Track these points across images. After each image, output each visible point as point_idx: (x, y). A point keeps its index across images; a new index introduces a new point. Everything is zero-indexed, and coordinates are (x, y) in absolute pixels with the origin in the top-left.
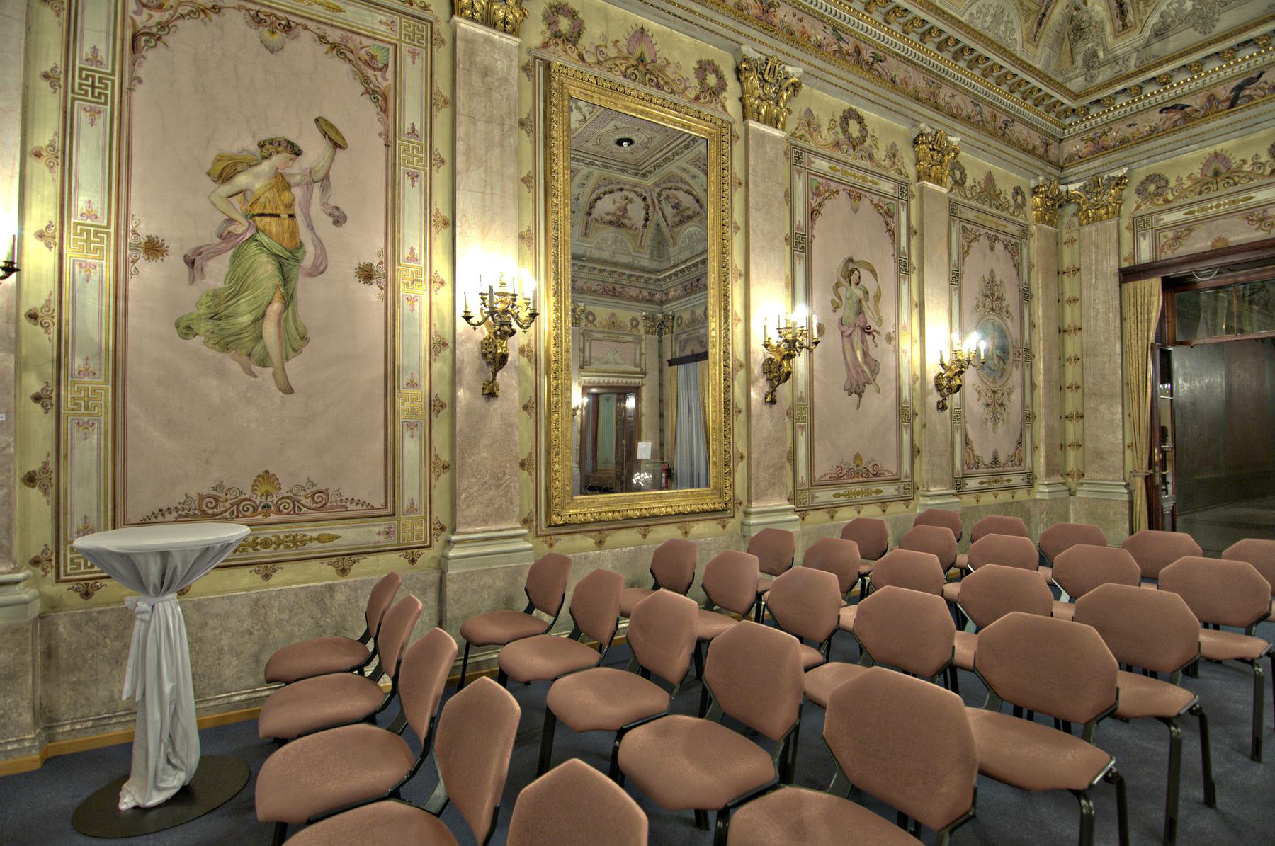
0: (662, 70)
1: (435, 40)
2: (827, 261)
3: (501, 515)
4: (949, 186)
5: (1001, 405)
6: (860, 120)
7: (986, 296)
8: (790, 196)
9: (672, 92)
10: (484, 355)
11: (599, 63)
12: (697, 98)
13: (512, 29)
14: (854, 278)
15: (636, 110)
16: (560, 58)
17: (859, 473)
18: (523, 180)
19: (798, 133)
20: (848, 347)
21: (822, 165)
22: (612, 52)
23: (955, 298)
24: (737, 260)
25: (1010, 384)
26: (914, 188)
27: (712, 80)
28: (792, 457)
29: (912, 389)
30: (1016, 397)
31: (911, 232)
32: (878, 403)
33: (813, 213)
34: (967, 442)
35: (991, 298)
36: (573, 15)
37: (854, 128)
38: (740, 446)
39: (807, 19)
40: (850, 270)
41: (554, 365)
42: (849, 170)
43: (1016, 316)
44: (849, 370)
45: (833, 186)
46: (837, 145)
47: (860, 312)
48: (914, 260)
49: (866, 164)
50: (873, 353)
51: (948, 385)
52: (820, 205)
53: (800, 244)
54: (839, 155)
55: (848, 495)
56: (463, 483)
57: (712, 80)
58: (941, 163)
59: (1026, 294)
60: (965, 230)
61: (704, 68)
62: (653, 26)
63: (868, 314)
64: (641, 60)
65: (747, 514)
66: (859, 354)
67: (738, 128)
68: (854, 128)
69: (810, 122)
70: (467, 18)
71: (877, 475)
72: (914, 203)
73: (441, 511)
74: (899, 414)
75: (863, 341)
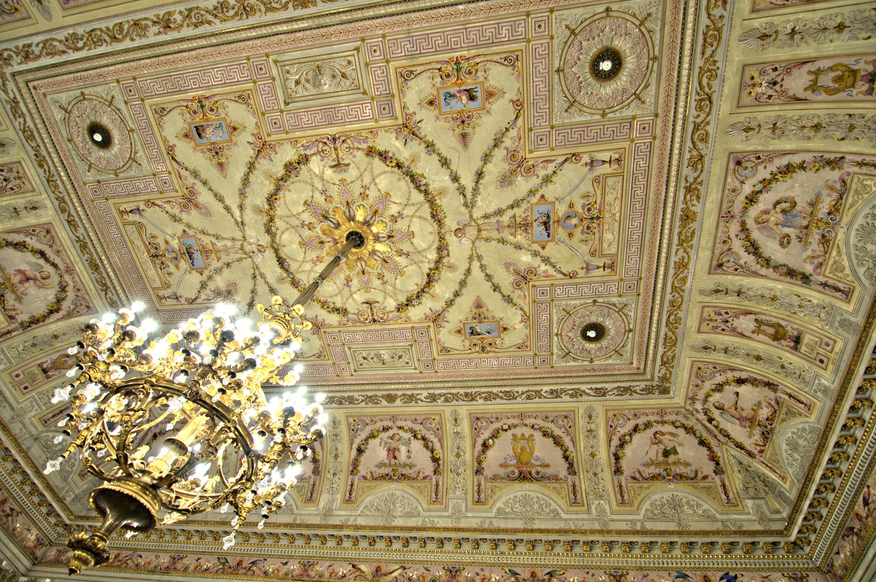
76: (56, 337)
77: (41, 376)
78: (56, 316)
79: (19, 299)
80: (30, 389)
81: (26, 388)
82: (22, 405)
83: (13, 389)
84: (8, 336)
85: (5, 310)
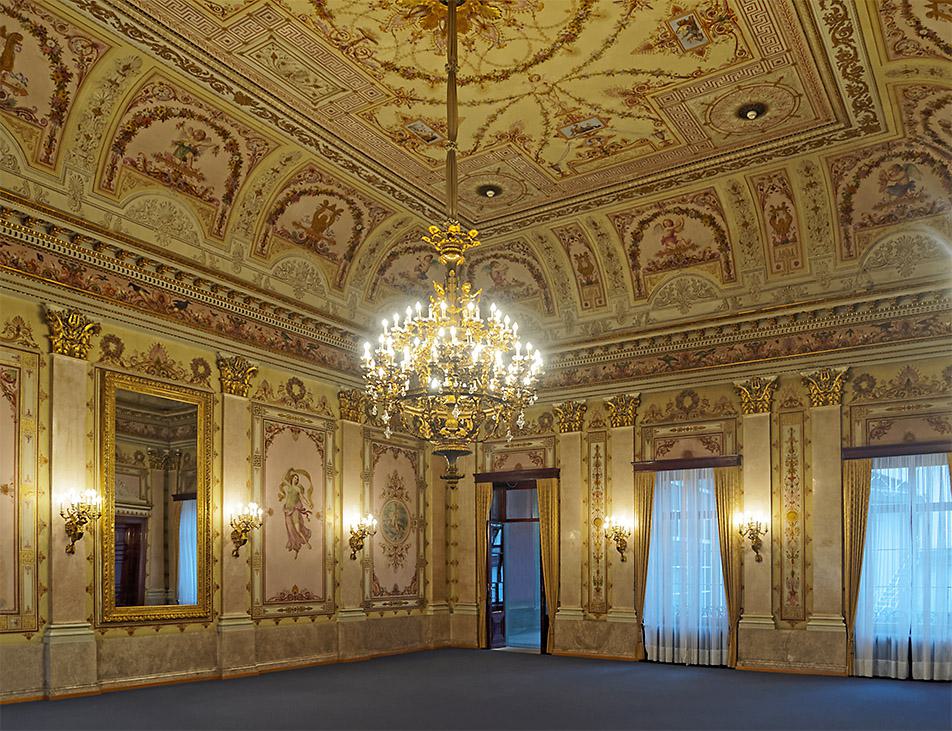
0: (170, 367)
1: (41, 364)
2: (275, 471)
3: (76, 616)
4: (363, 422)
5: (401, 555)
6: (300, 384)
7: (391, 487)
8: (251, 434)
9: (177, 379)
10: (67, 531)
11: (132, 366)
12: (192, 381)
13: (82, 356)
14: (294, 480)
15: (155, 393)
16: (109, 365)
17: (295, 600)
18: (88, 435)
19: (258, 396)
20: (289, 521)
21: (274, 414)
22: (141, 360)
23: (367, 489)
24: (216, 472)
25: (407, 542)
26: (338, 423)
27: (201, 369)
28: (250, 587)
29: (334, 546)
30: (413, 550)
31: (335, 450)
32: (311, 554)
33: (267, 443)
34: (374, 578)
35: (395, 488)
36: (117, 341)
37: (296, 390)
38: (217, 580)
39: (264, 328)
40: (291, 476)
41: (105, 536)
42: (292, 415)
43: (414, 500)
44: (289, 536)
45: (281, 425)
46: (284, 400)
47: (298, 500)
48: (337, 468)
49: (306, 411)
50: (306, 525)
51: (357, 543)
52: (272, 437)
53: (258, 461)
54: (285, 406)
55: (288, 610)
56: (55, 599)
57: (201, 369)
58: (356, 408)
59: (421, 485)
60: (375, 446)
61: (197, 363)
62: (164, 341)
63: (304, 501)
64: (158, 362)
65: (220, 620)
66: (297, 526)
67: (218, 396)
68: (296, 390)
69: (265, 388)
70: (59, 353)
71: (308, 598)
72: (338, 432)
73: (43, 613)
74: (324, 560)
75: (300, 518)
76: (746, 225)
77: (790, 247)
78: (718, 220)
79: (694, 247)
80: (799, 260)
81: (796, 264)
82: (814, 272)
83: (792, 275)
84: (731, 264)
85: (702, 259)
